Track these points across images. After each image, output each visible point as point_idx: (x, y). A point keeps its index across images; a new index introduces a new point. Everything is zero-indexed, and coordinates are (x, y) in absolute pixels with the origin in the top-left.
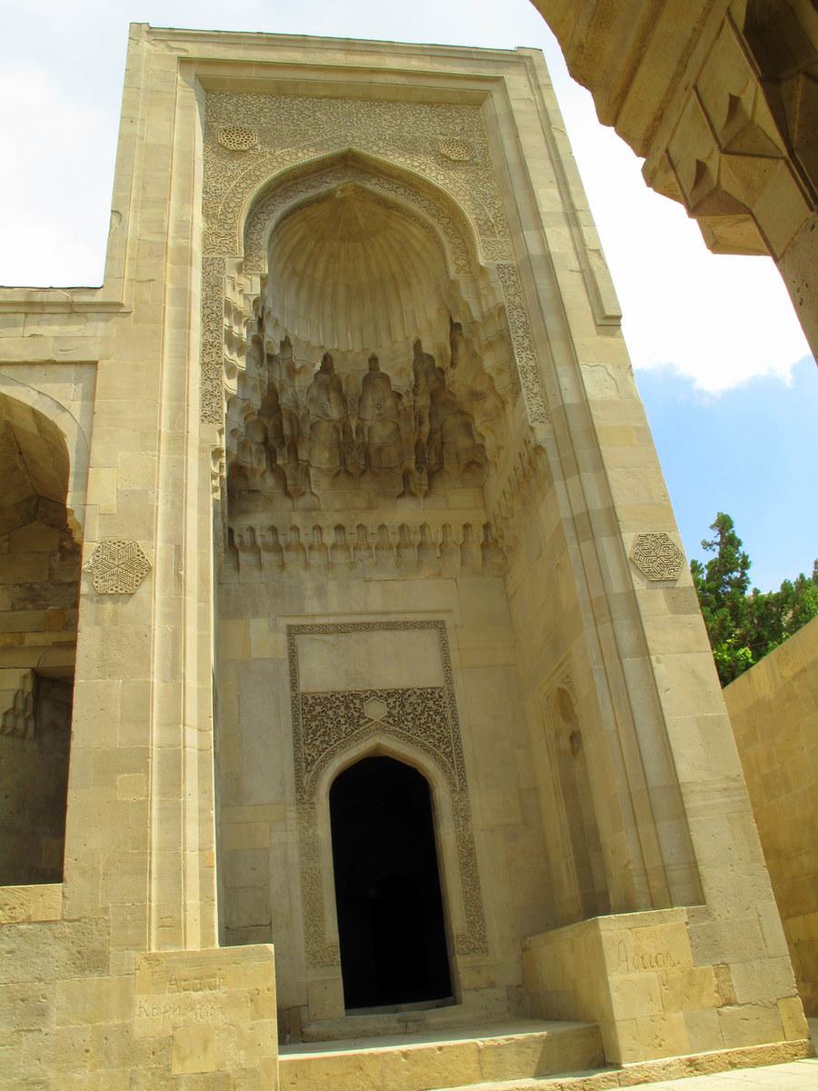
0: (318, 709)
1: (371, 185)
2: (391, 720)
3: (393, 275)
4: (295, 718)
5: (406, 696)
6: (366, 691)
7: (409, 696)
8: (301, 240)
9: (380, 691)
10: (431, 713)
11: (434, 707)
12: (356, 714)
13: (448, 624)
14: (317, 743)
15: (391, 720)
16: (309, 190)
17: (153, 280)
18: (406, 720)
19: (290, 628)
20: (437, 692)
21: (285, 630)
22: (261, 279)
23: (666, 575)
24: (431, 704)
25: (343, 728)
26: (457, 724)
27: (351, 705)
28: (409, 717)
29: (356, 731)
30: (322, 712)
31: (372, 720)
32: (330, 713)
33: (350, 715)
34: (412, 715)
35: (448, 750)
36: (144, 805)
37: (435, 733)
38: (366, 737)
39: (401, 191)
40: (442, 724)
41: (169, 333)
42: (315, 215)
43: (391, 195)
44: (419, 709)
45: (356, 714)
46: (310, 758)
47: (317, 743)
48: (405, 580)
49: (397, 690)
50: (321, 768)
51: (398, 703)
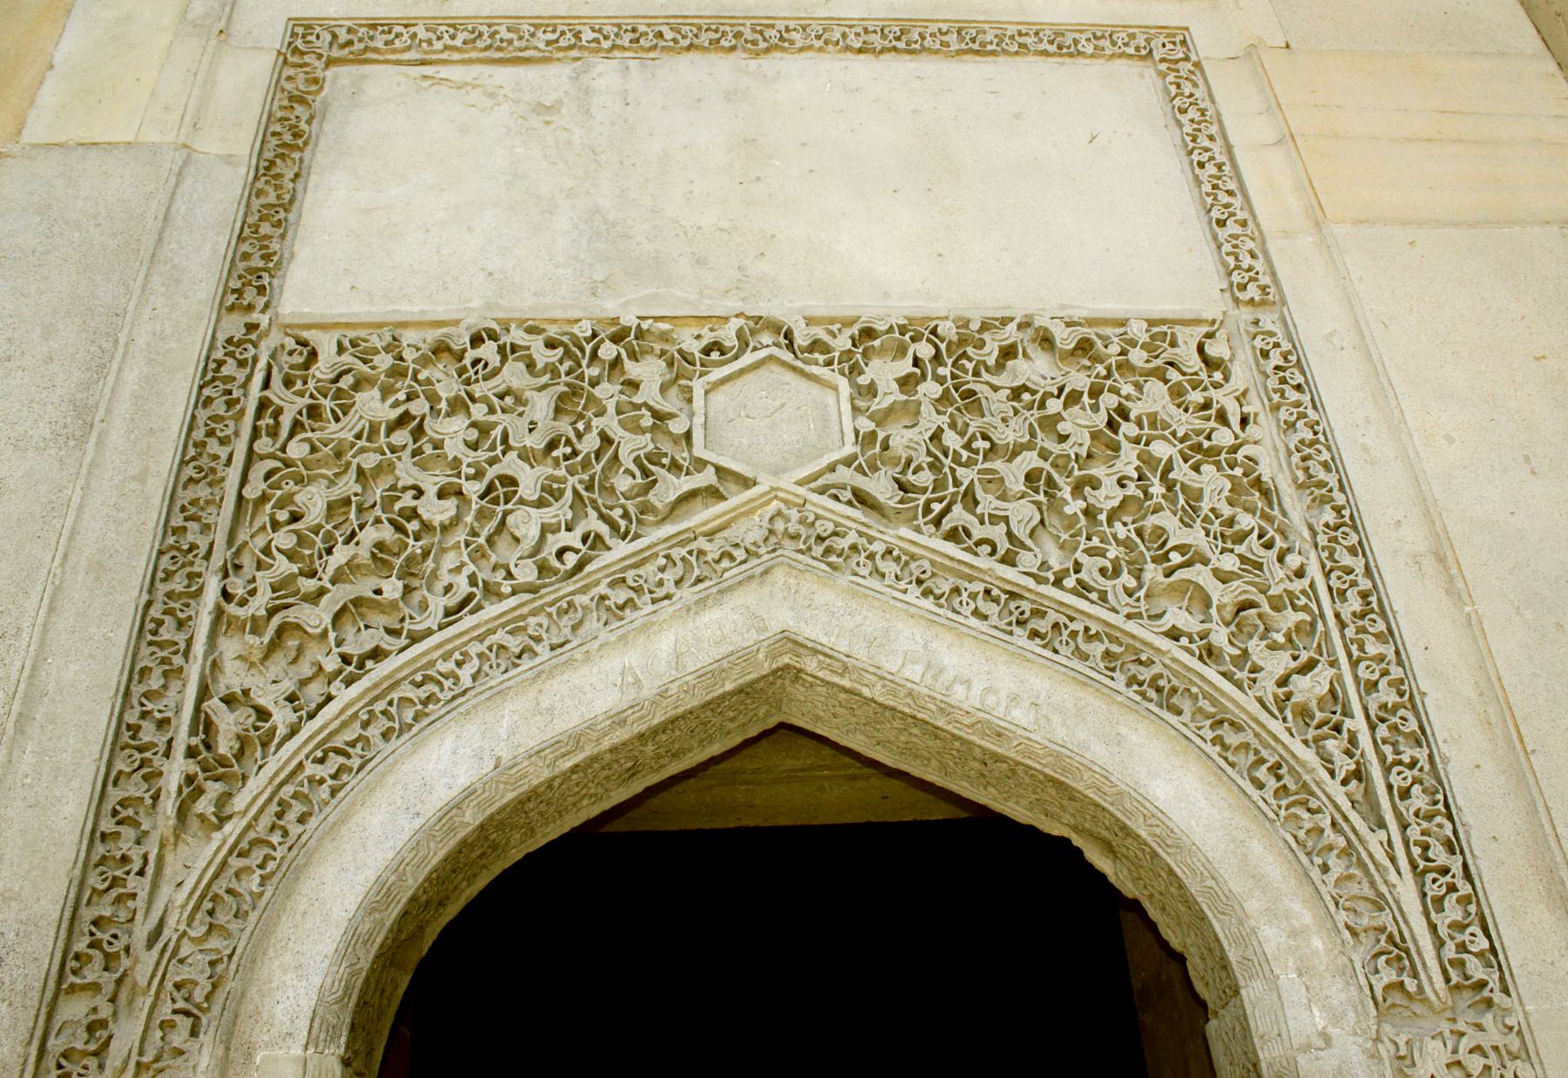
0: (372, 406)
10: (1161, 450)
11: (1184, 422)
12: (631, 446)
13: (1205, 45)
15: (881, 487)
18: (994, 482)
20: (1188, 339)
24: (1156, 397)
25: (527, 524)
26: (1348, 522)
28: (1014, 473)
31: (747, 483)
34: (1029, 460)
35: (1310, 688)
37: (1201, 575)
38: (687, 594)
40: (1246, 521)
44: (1080, 424)
47: (316, 617)
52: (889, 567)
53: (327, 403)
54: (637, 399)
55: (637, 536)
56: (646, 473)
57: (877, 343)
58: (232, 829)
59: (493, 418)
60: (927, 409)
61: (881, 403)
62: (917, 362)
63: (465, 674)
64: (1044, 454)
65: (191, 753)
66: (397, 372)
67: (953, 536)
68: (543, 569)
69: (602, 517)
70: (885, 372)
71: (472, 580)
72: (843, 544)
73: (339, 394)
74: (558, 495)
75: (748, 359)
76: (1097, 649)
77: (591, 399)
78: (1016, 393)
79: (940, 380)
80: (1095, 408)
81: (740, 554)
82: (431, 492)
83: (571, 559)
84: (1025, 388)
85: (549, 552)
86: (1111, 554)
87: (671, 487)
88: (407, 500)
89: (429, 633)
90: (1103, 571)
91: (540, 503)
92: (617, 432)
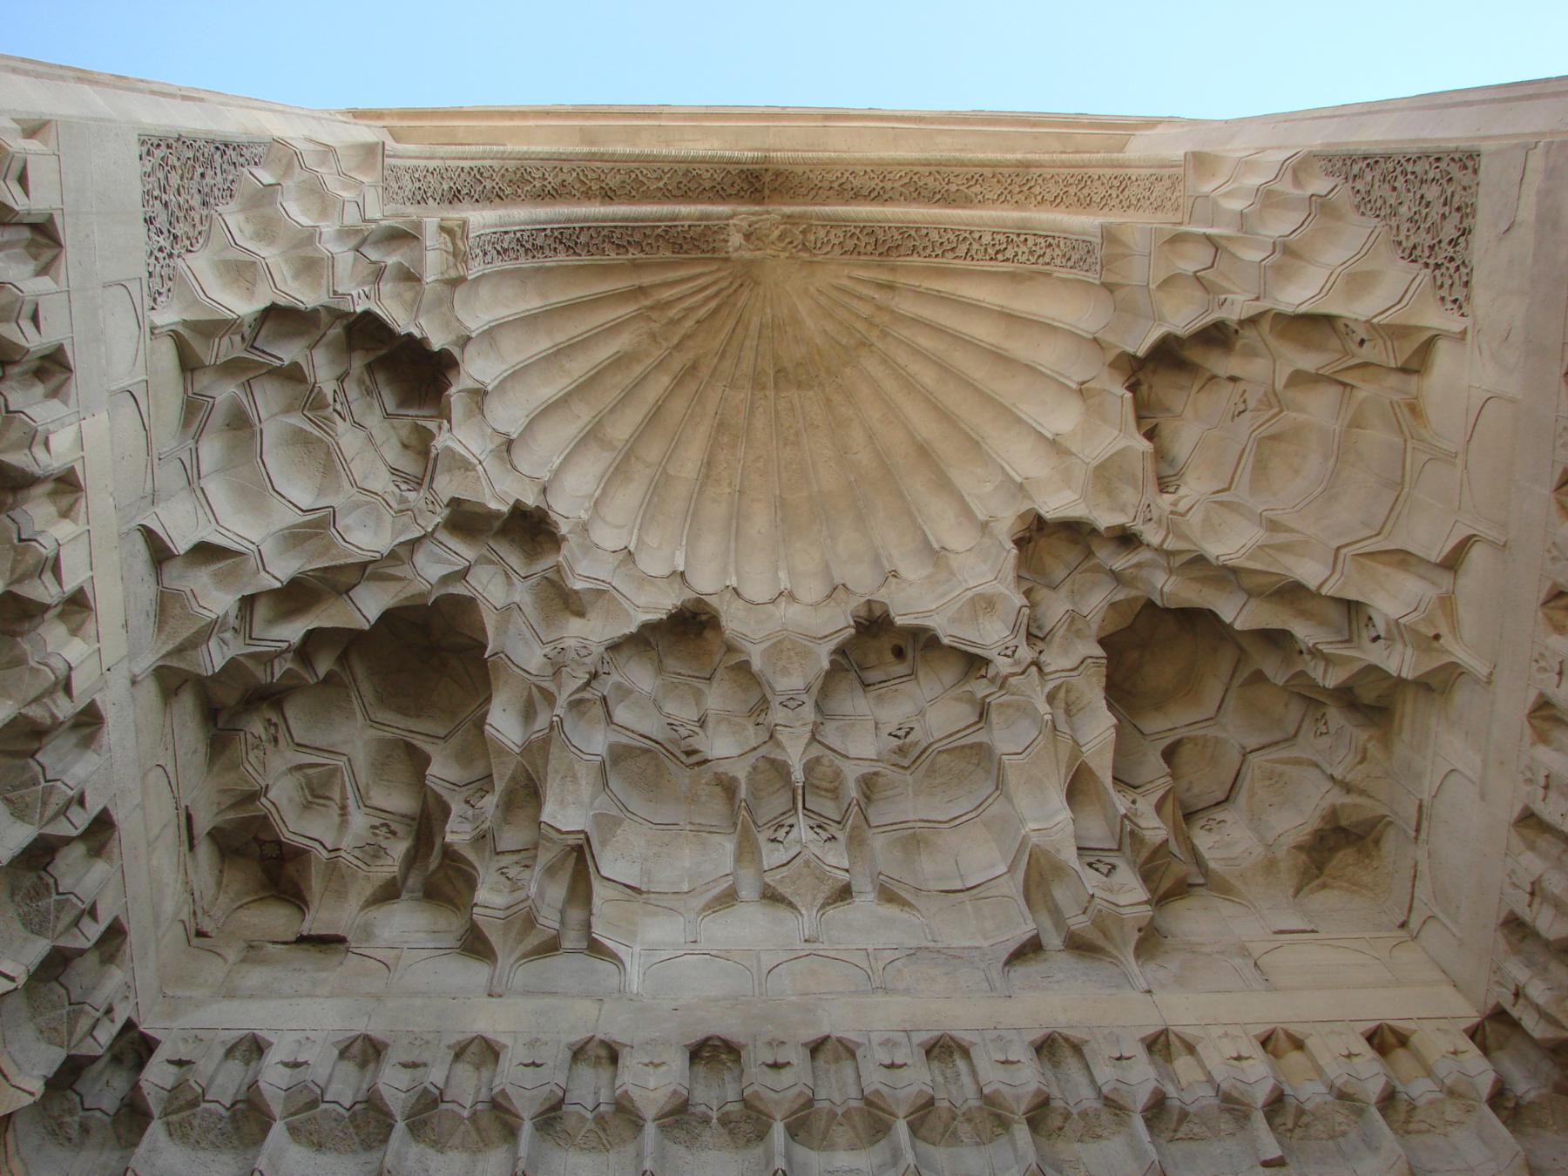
3: (924, 452)
8: (620, 362)
42: (667, 294)
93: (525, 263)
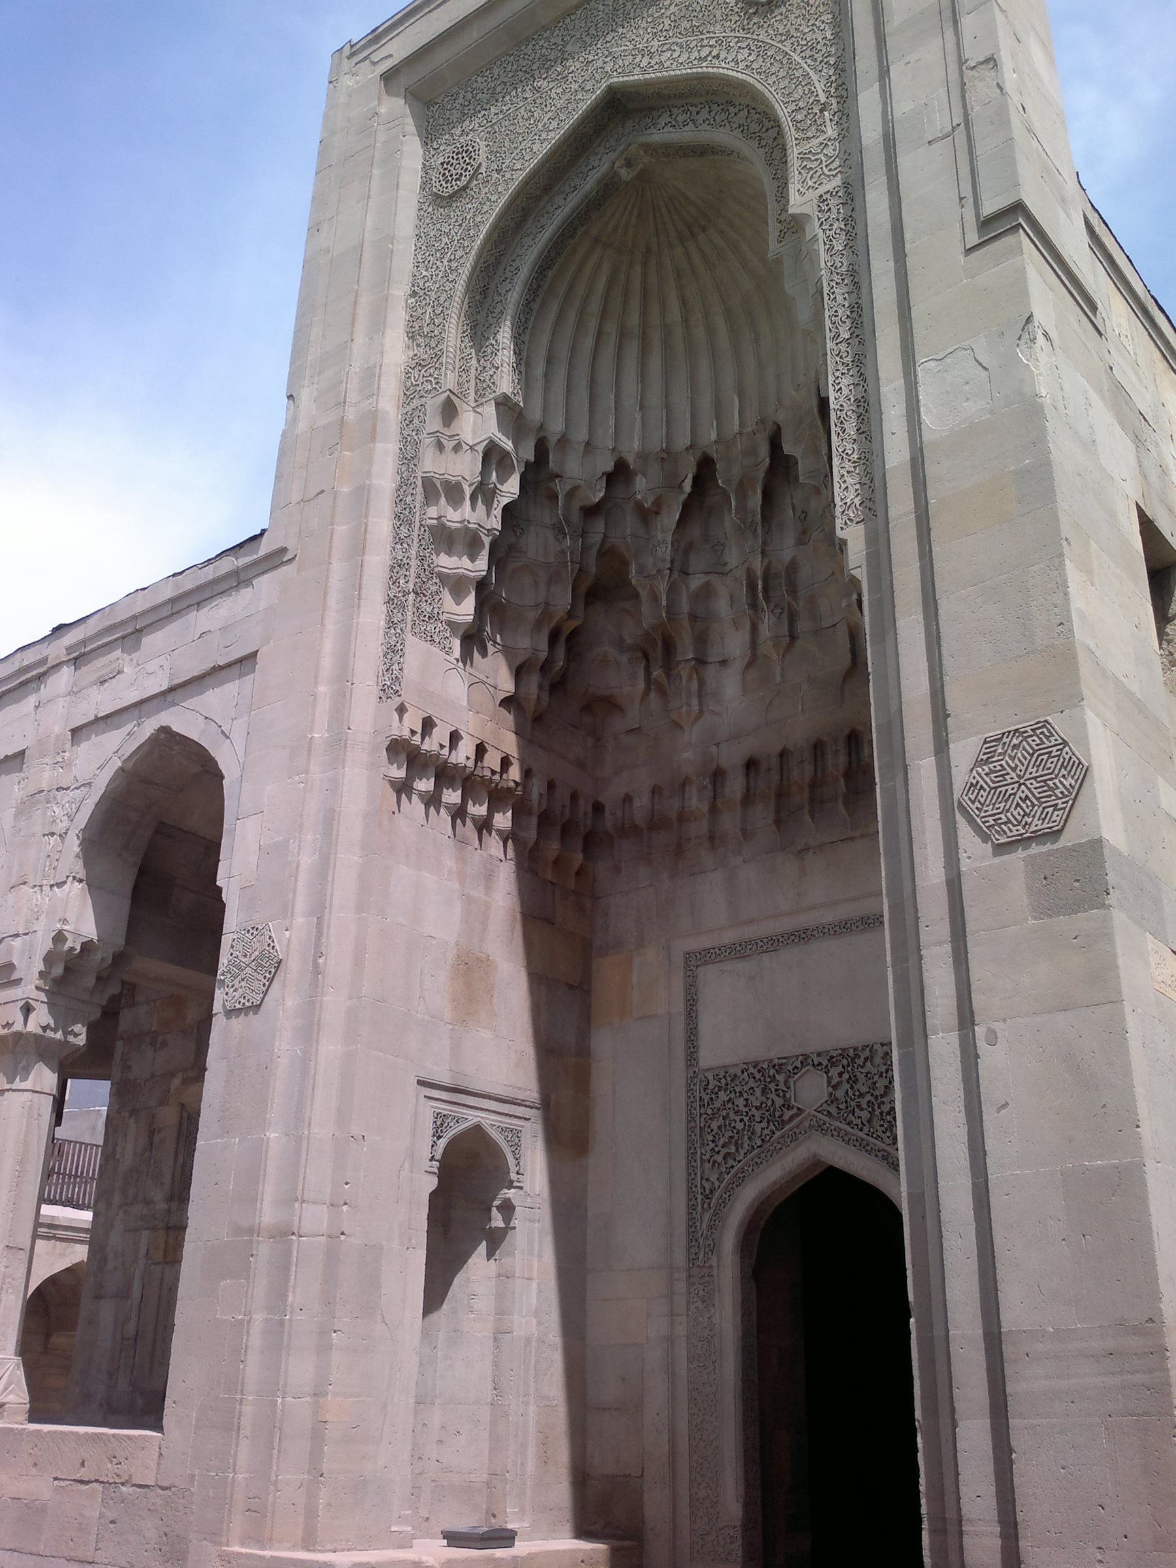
1: (663, 133)
2: (833, 1110)
4: (690, 1118)
5: (860, 1061)
6: (797, 1057)
7: (866, 1059)
8: (611, 284)
9: (819, 1055)
12: (779, 1102)
14: (719, 1158)
15: (833, 1110)
16: (570, 198)
17: (322, 491)
18: (859, 1106)
19: (688, 956)
21: (678, 958)
22: (497, 404)
23: (1037, 825)
27: (772, 1086)
29: (778, 1134)
30: (730, 1099)
32: (740, 1102)
33: (770, 1102)
34: (869, 1097)
36: (242, 1327)
39: (704, 114)
41: (338, 568)
42: (611, 226)
43: (687, 135)
45: (779, 1102)
46: (707, 1186)
48: (862, 836)
49: (843, 1050)
50: (723, 1203)
51: (846, 1076)
52: (835, 1133)
53: (713, 1096)
54: (779, 1088)
55: (782, 1129)
56: (782, 1110)
57: (834, 1060)
58: (712, 1211)
59: (749, 1097)
60: (845, 1083)
61: (834, 1082)
62: (843, 1067)
63: (750, 1170)
64: (872, 1095)
65: (702, 1193)
66: (727, 1084)
67: (849, 1124)
68: (763, 1140)
69: (774, 1125)
70: (834, 1072)
71: (749, 1145)
72: (825, 1127)
73: (716, 1093)
74: (764, 1118)
75: (803, 1071)
76: (880, 1154)
77: (770, 1089)
78: (867, 1073)
79: (848, 1072)
80: (886, 1077)
81: (803, 1132)
82: (738, 1121)
83: (768, 1137)
84: (869, 1073)
85: (763, 1137)
86: (885, 1126)
87: (788, 1114)
88: (733, 1125)
89: (741, 1160)
90: (883, 1132)
91: (761, 1122)
92: (776, 1098)
93: (536, 306)
